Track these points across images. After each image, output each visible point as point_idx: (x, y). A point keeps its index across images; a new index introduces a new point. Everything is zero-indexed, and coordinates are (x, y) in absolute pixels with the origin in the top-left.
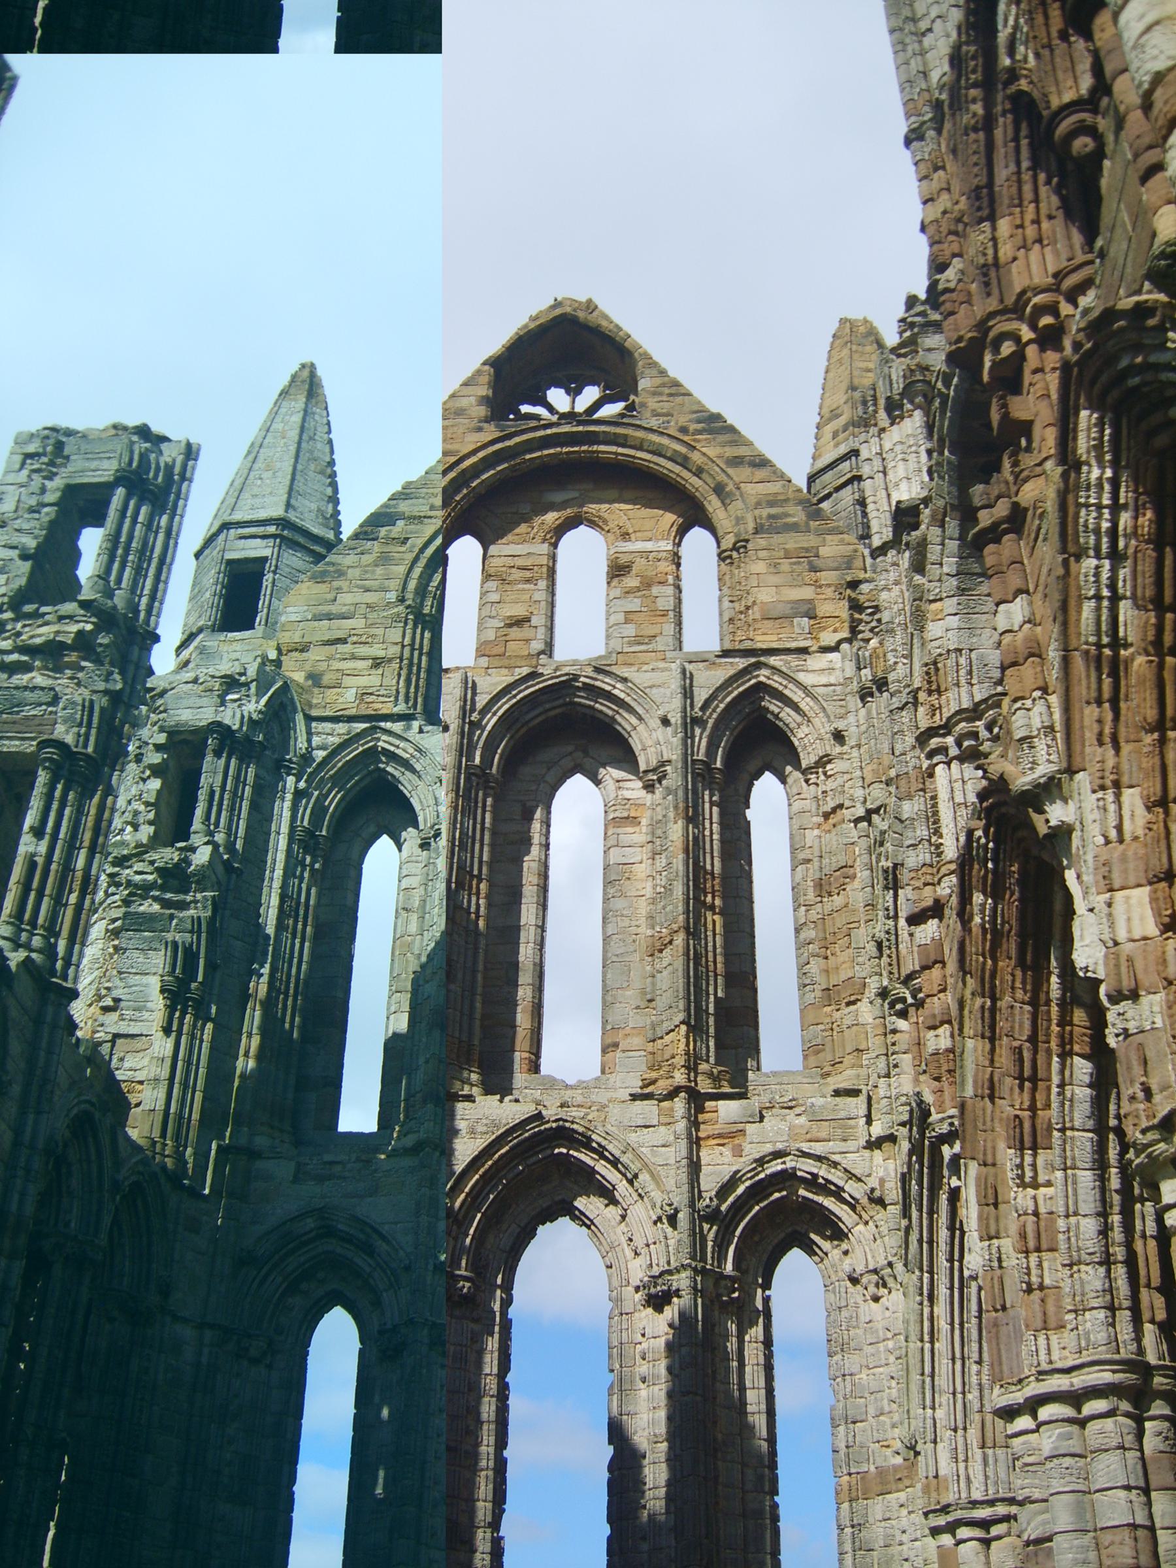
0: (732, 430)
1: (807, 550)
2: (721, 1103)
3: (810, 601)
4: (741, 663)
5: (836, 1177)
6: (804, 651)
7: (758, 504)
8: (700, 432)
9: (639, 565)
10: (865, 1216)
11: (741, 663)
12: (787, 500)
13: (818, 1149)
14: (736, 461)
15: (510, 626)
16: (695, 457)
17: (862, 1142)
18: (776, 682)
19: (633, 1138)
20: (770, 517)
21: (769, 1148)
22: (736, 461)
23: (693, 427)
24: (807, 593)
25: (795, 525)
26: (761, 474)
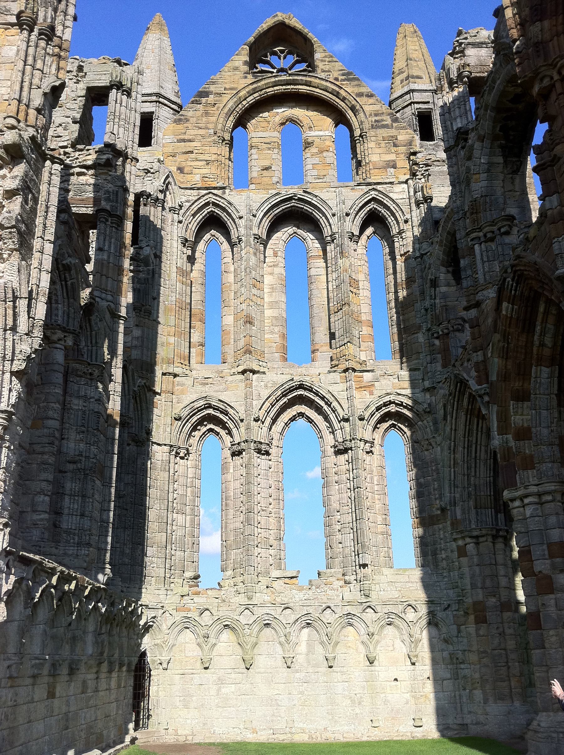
1: (392, 137)
2: (365, 374)
3: (394, 161)
4: (365, 188)
6: (391, 183)
7: (371, 115)
8: (344, 80)
10: (422, 419)
12: (383, 113)
15: (263, 170)
16: (342, 92)
17: (421, 389)
20: (376, 121)
23: (340, 78)
24: (392, 157)
25: (387, 124)
26: (371, 100)
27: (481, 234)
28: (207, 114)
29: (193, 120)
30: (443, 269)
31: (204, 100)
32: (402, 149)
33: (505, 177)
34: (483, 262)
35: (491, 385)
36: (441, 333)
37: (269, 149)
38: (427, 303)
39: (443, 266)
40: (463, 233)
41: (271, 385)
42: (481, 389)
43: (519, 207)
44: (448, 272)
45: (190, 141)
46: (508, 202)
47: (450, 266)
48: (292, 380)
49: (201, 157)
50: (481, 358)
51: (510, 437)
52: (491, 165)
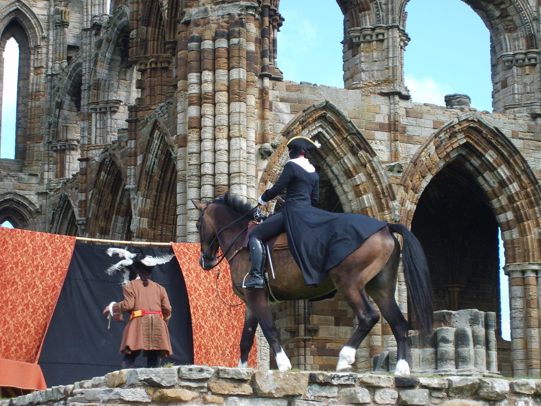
10: (34, 216)
13: (21, 193)
27: (98, 107)
30: (68, 97)
33: (121, 70)
34: (96, 128)
35: (87, 220)
36: (59, 148)
38: (51, 119)
39: (69, 95)
40: (86, 102)
42: (80, 220)
43: (127, 92)
44: (72, 100)
46: (120, 87)
47: (74, 96)
50: (83, 198)
52: (112, 60)
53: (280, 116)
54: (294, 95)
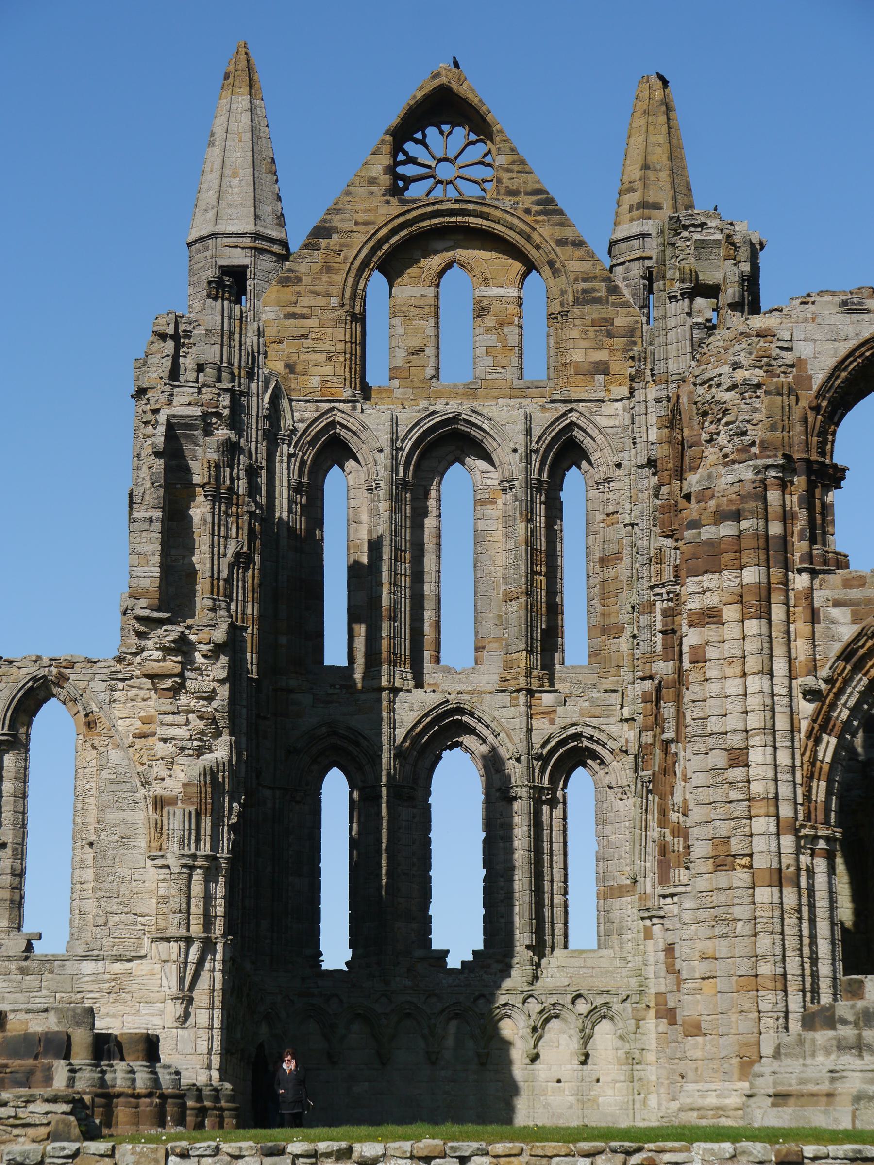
0: (560, 212)
1: (606, 320)
3: (606, 363)
4: (562, 408)
5: (603, 738)
7: (576, 280)
8: (538, 214)
9: (496, 306)
11: (562, 408)
12: (595, 277)
13: (594, 722)
14: (562, 242)
15: (412, 354)
16: (535, 236)
17: (618, 718)
18: (582, 422)
19: (497, 713)
20: (584, 291)
21: (569, 721)
22: (562, 242)
24: (602, 355)
25: (600, 298)
26: (579, 253)
27: (664, 591)
28: (328, 269)
29: (307, 280)
31: (323, 242)
32: (619, 342)
37: (422, 318)
41: (418, 708)
45: (303, 317)
48: (447, 701)
49: (320, 346)
51: (667, 831)
53: (834, 629)
54: (855, 593)
